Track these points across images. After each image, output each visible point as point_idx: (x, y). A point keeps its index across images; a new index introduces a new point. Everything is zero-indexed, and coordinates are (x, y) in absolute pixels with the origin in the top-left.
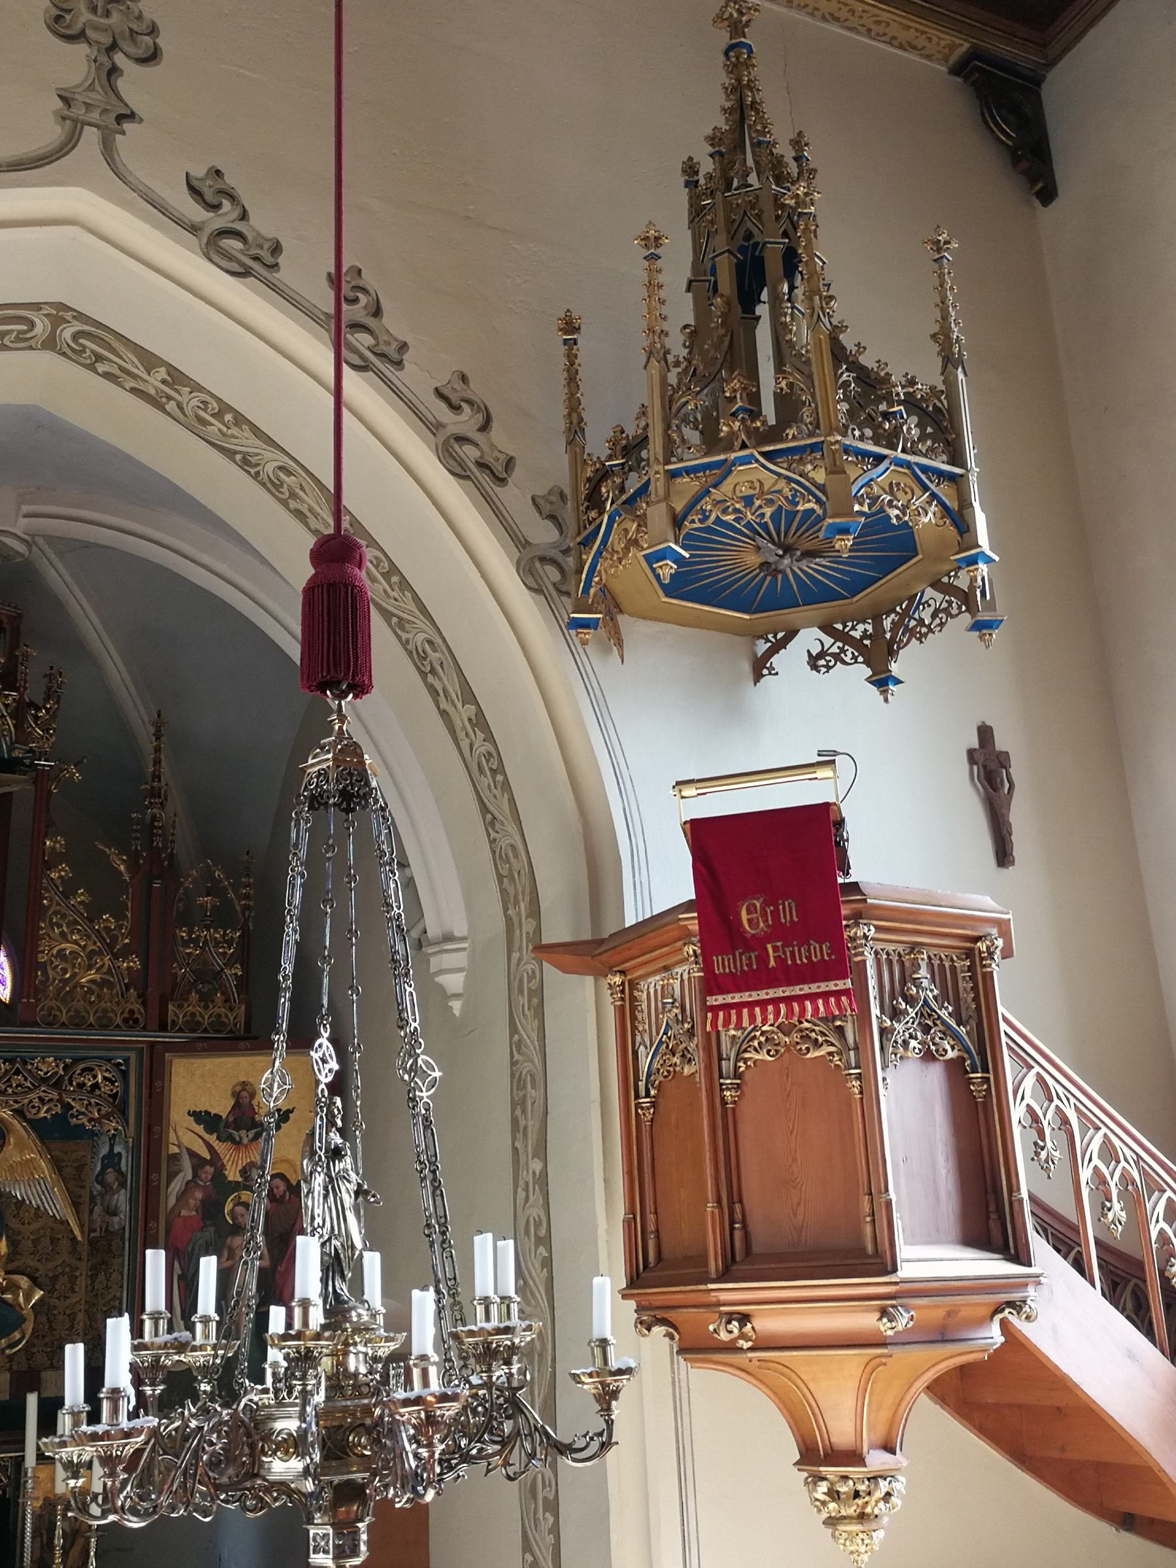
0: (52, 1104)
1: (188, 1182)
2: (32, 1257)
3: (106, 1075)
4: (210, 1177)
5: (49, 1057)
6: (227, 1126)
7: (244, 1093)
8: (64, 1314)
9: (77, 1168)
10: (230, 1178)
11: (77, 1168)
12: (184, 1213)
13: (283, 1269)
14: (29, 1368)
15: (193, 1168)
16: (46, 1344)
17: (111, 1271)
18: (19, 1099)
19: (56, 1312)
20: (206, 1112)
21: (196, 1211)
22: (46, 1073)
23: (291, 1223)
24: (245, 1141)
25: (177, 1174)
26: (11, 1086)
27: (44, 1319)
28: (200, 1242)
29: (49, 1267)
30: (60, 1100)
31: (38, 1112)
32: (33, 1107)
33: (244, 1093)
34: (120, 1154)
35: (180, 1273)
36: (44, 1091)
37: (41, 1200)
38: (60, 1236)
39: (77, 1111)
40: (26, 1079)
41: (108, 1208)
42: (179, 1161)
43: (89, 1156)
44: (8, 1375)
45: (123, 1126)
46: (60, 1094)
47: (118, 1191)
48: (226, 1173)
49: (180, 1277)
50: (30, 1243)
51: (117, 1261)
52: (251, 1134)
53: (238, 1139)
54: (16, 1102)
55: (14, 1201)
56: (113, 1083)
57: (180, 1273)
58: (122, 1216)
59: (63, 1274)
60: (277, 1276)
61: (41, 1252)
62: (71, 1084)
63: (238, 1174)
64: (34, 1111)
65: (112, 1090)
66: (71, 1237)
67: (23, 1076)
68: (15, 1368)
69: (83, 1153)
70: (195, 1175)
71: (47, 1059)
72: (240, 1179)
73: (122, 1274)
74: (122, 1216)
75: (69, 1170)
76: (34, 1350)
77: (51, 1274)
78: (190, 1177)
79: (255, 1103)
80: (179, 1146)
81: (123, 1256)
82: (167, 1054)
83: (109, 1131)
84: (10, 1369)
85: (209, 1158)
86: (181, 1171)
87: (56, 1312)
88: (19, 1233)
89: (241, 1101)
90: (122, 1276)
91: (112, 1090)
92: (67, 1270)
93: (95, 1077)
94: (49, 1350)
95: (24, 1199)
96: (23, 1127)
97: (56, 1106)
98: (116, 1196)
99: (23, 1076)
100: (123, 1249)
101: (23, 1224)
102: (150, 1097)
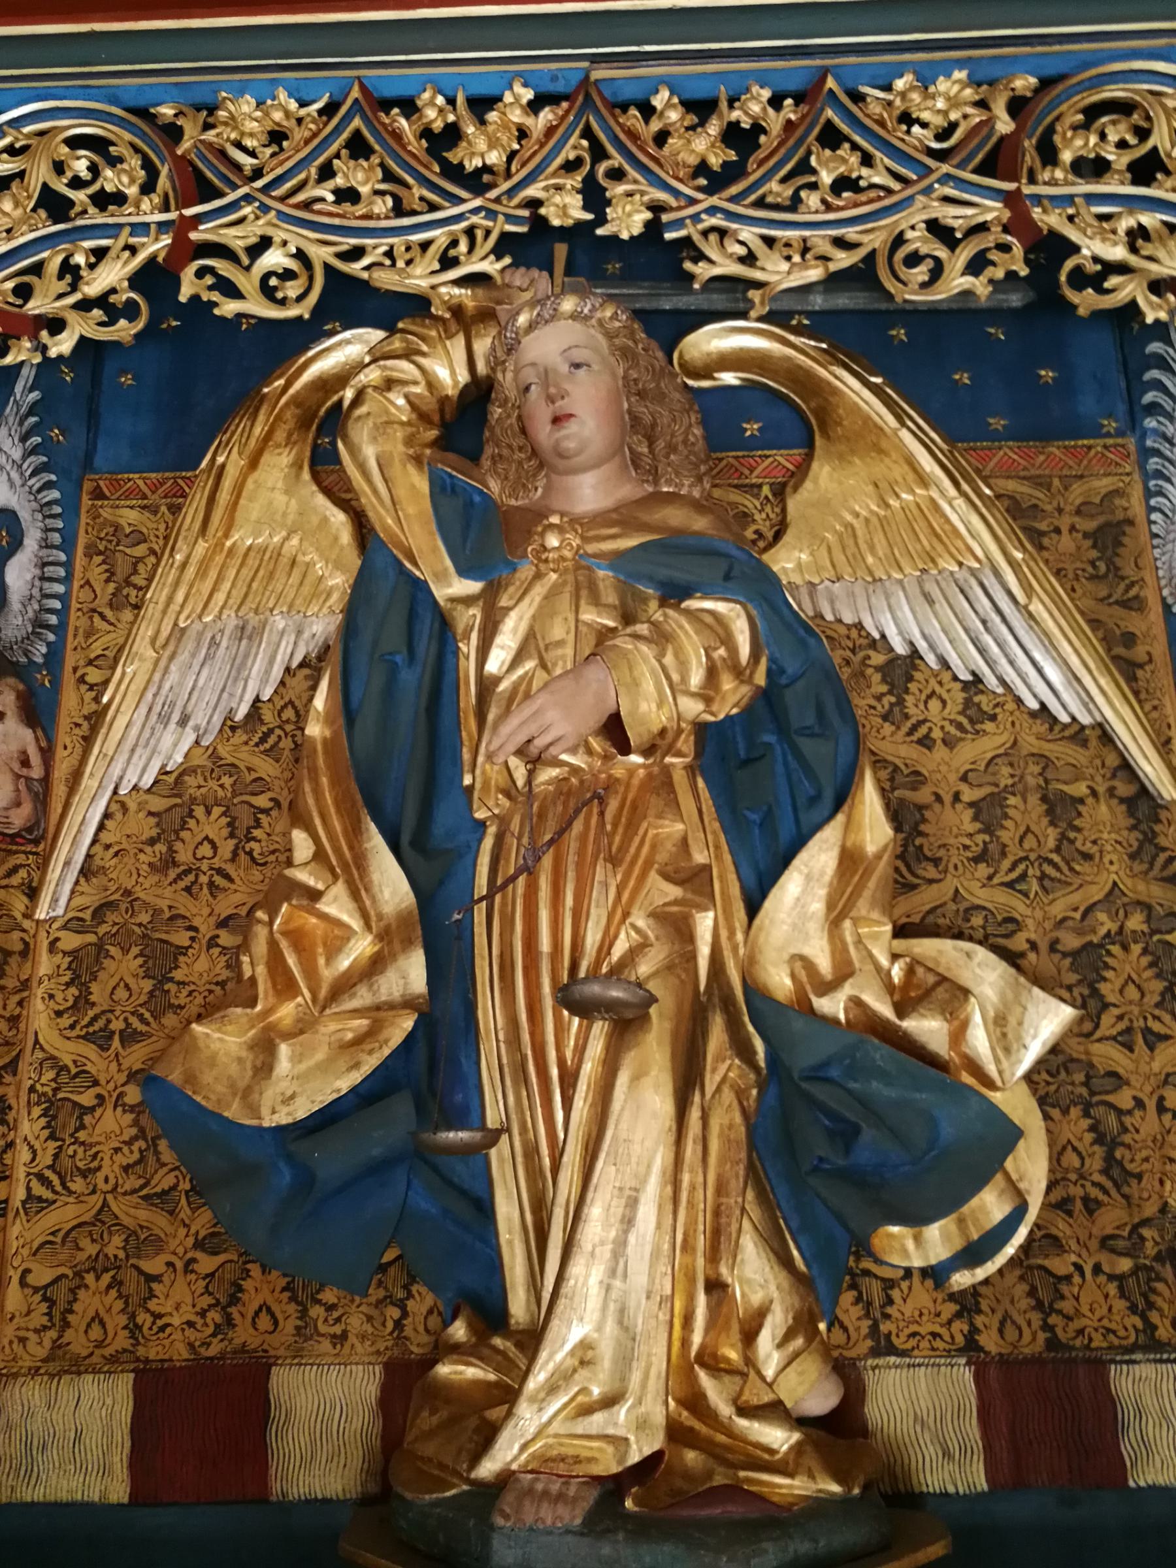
0: (988, 240)
2: (983, 870)
5: (946, 69)
8: (1161, 1108)
9: (1095, 537)
11: (1095, 537)
14: (1053, 1343)
16: (1106, 1242)
18: (851, 233)
19: (1124, 1099)
22: (942, 136)
26: (814, 186)
27: (1076, 1127)
29: (1058, 909)
30: (1019, 223)
31: (937, 271)
32: (914, 259)
36: (947, 200)
37: (982, 651)
38: (1080, 789)
39: (1096, 259)
40: (867, 160)
43: (1137, 493)
44: (967, 1375)
46: (1011, 200)
50: (966, 820)
54: (840, 243)
55: (878, 659)
59: (1120, 937)
61: (1014, 852)
62: (1049, 155)
64: (920, 273)
66: (1125, 789)
67: (855, 147)
68: (989, 1341)
69: (1104, 484)
71: (942, 85)
75: (1066, 542)
76: (1060, 1265)
77: (1071, 942)
84: (971, 1347)
87: (1124, 1099)
88: (917, 779)
92: (1136, 922)
93: (1143, 134)
94: (1125, 1265)
95: (915, 654)
96: (875, 390)
97: (1005, 248)
99: (855, 147)
101: (926, 742)
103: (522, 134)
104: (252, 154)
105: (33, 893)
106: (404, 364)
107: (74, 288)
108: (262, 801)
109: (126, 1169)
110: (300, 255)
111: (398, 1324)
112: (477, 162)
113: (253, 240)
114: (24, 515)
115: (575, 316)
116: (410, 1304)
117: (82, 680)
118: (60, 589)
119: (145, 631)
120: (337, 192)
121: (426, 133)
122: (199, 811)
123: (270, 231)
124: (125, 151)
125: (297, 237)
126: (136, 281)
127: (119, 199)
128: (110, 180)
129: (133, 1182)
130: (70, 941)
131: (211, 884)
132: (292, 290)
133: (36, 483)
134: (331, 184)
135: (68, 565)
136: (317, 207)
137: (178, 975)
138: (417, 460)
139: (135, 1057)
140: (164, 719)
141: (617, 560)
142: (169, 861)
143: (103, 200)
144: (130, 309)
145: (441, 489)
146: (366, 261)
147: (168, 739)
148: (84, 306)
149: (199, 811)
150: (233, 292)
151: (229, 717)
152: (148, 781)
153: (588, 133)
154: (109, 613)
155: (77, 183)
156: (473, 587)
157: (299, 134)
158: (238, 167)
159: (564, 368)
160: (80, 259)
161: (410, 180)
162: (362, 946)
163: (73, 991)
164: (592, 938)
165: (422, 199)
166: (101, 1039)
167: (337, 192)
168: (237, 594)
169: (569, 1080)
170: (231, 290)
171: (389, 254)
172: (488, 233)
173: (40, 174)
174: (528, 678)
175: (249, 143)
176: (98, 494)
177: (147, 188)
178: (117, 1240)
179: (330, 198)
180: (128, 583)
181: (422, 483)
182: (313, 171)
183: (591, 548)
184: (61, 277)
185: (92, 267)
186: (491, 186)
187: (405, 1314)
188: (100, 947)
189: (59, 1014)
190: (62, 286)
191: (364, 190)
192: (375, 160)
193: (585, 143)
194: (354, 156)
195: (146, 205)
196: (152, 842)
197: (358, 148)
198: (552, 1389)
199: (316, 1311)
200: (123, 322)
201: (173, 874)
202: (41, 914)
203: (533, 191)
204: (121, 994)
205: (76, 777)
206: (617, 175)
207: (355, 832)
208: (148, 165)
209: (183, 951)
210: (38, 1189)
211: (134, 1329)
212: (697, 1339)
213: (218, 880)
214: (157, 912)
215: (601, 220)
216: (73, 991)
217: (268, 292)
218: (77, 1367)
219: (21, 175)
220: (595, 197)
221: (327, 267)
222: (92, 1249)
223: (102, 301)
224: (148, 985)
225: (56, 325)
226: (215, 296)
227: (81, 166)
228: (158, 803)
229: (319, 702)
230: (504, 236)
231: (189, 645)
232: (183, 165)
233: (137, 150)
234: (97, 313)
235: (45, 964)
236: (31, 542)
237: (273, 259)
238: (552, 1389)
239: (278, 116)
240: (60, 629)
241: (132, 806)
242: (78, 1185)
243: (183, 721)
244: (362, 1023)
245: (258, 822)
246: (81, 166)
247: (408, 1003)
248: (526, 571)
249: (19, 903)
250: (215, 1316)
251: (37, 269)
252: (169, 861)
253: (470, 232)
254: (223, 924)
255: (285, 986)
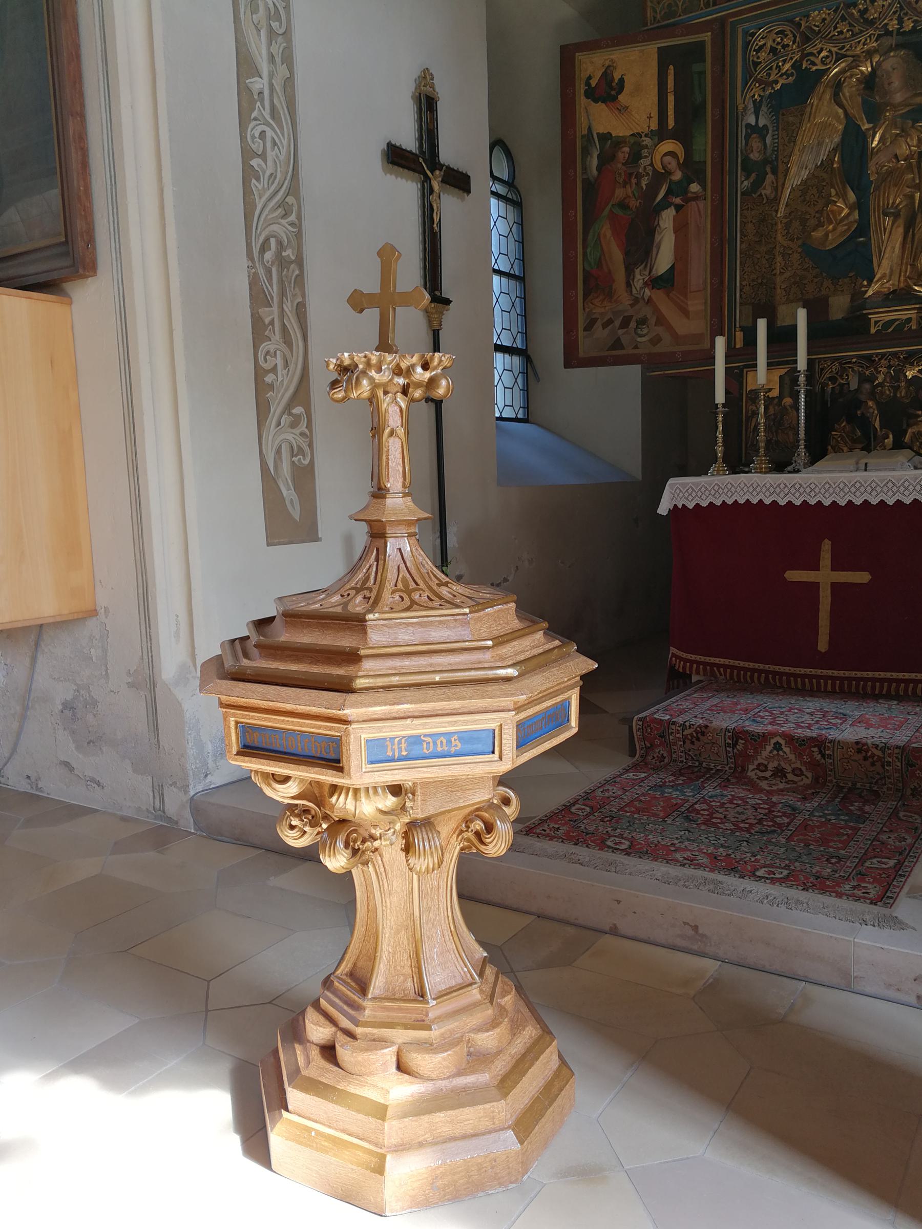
103: (883, 6)
104: (817, 26)
105: (777, 211)
106: (855, 70)
107: (779, 71)
108: (824, 184)
109: (799, 265)
110: (830, 51)
111: (854, 287)
112: (872, 17)
113: (819, 50)
114: (768, 125)
115: (893, 56)
116: (857, 283)
117: (783, 162)
118: (777, 141)
119: (797, 148)
120: (838, 32)
121: (860, 11)
122: (810, 188)
123: (823, 46)
124: (789, 33)
125: (830, 46)
126: (793, 66)
127: (788, 45)
128: (786, 41)
129: (800, 267)
130: (784, 221)
131: (814, 204)
132: (828, 60)
133: (770, 116)
134: (836, 31)
135: (778, 134)
136: (834, 38)
137: (807, 224)
138: (859, 95)
139: (800, 242)
140: (802, 168)
141: (902, 116)
142: (804, 200)
143: (784, 47)
144: (792, 75)
145: (864, 102)
146: (845, 49)
147: (803, 173)
148: (781, 76)
149: (810, 188)
150: (814, 64)
151: (816, 165)
152: (799, 183)
153: (899, 3)
154: (788, 144)
155: (778, 44)
156: (871, 125)
157: (828, 19)
158: (815, 31)
159: (891, 70)
160: (780, 64)
161: (856, 25)
162: (846, 211)
163: (786, 231)
164: (891, 201)
165: (859, 29)
166: (792, 240)
167: (838, 32)
168: (817, 134)
169: (885, 229)
170: (814, 64)
171: (851, 47)
172: (875, 35)
173: (770, 43)
174: (881, 146)
175: (817, 24)
176: (783, 115)
177: (794, 42)
178: (798, 278)
179: (836, 34)
180: (792, 136)
181: (860, 99)
182: (832, 29)
183: (896, 114)
184: (776, 69)
185: (783, 65)
186: (876, 23)
187: (855, 285)
188: (791, 221)
189: (783, 236)
190: (776, 71)
191: (845, 31)
192: (847, 22)
193: (898, 5)
194: (842, 22)
195: (794, 47)
196: (800, 196)
197: (843, 19)
198: (878, 281)
199: (837, 286)
200: (790, 78)
201: (805, 203)
202: (778, 216)
203: (885, 22)
204: (796, 230)
205: (783, 185)
206: (906, 14)
207: (844, 187)
208: (795, 37)
209: (808, 219)
210: (782, 271)
211: (802, 293)
212: (908, 274)
213: (815, 203)
214: (802, 212)
215: (902, 27)
216: (786, 231)
217: (823, 63)
218: (792, 302)
219: (765, 44)
220: (900, 21)
221: (836, 52)
222: (793, 280)
223: (785, 73)
224: (801, 227)
225: (776, 82)
226: (811, 66)
227: (779, 40)
228: (801, 188)
229: (836, 159)
230: (878, 34)
231: (807, 149)
232: (803, 34)
233: (792, 32)
234: (785, 77)
235: (779, 226)
236: (770, 132)
237: (824, 54)
238: (878, 281)
239: (824, 16)
240: (777, 151)
241: (796, 189)
242: (790, 269)
243: (806, 169)
244: (846, 227)
245: (823, 189)
246: (779, 40)
247: (855, 221)
248: (882, 122)
249: (774, 214)
250: (818, 289)
251: (771, 68)
252: (804, 200)
253: (870, 36)
254: (817, 212)
255: (830, 222)
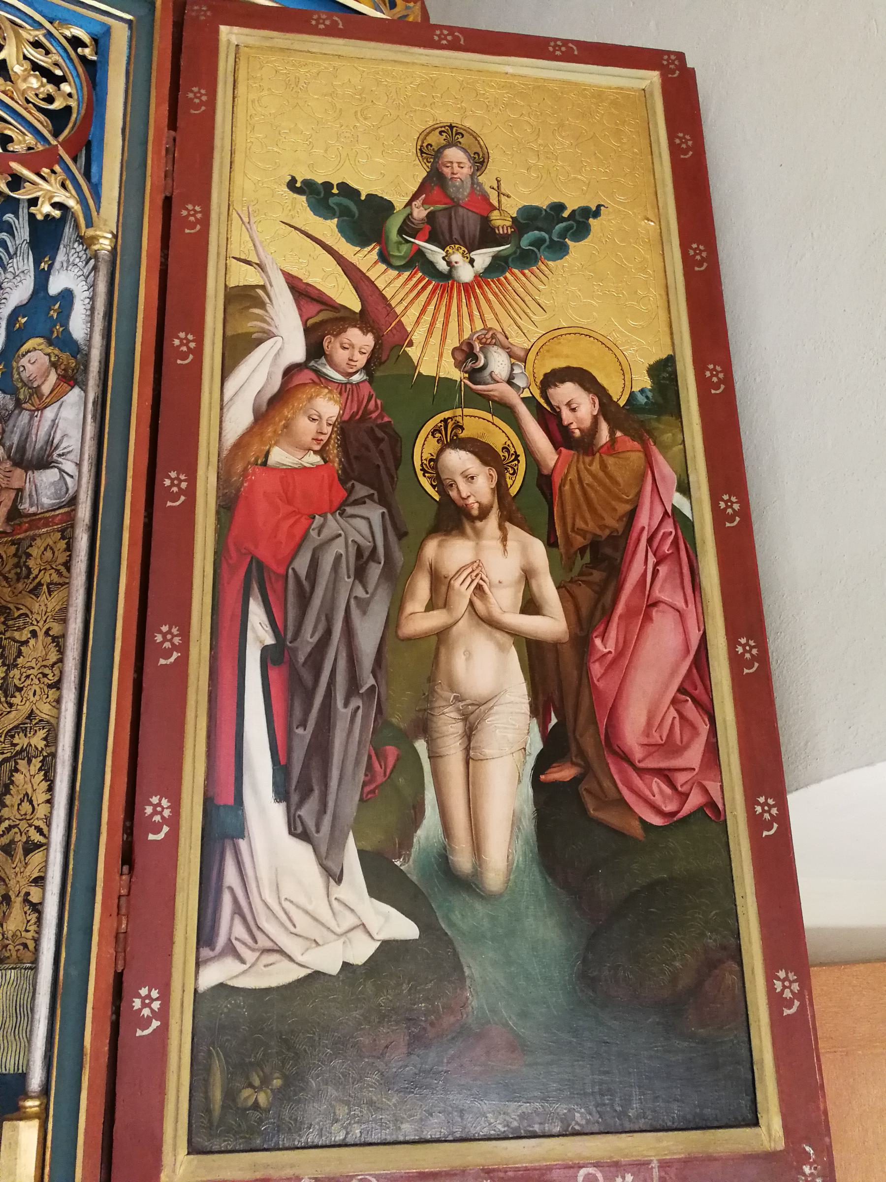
1: (290, 371)
3: (37, 56)
4: (361, 360)
6: (408, 229)
7: (454, 154)
10: (427, 369)
12: (280, 456)
13: (611, 647)
15: (307, 331)
17: (25, 635)
20: (343, 186)
21: (320, 453)
23: (628, 507)
24: (466, 273)
25: (259, 342)
28: (338, 547)
33: (454, 154)
34: (67, 296)
35: (270, 640)
41: (22, 448)
42: (262, 305)
45: (82, 201)
47: (57, 395)
48: (413, 352)
49: (268, 657)
51: (46, 604)
52: (483, 257)
53: (442, 266)
56: (57, 81)
57: (270, 640)
58: (69, 467)
60: (596, 669)
63: (448, 361)
65: (50, 99)
70: (315, 350)
72: (456, 375)
73: (59, 641)
74: (69, 467)
78: (297, 352)
79: (486, 180)
80: (261, 266)
81: (65, 585)
82: (224, 30)
83: (33, 202)
85: (356, 306)
86: (269, 335)
89: (447, 171)
90: (61, 650)
91: (50, 99)
98: (49, 413)
100: (68, 565)
102: (173, 124)
